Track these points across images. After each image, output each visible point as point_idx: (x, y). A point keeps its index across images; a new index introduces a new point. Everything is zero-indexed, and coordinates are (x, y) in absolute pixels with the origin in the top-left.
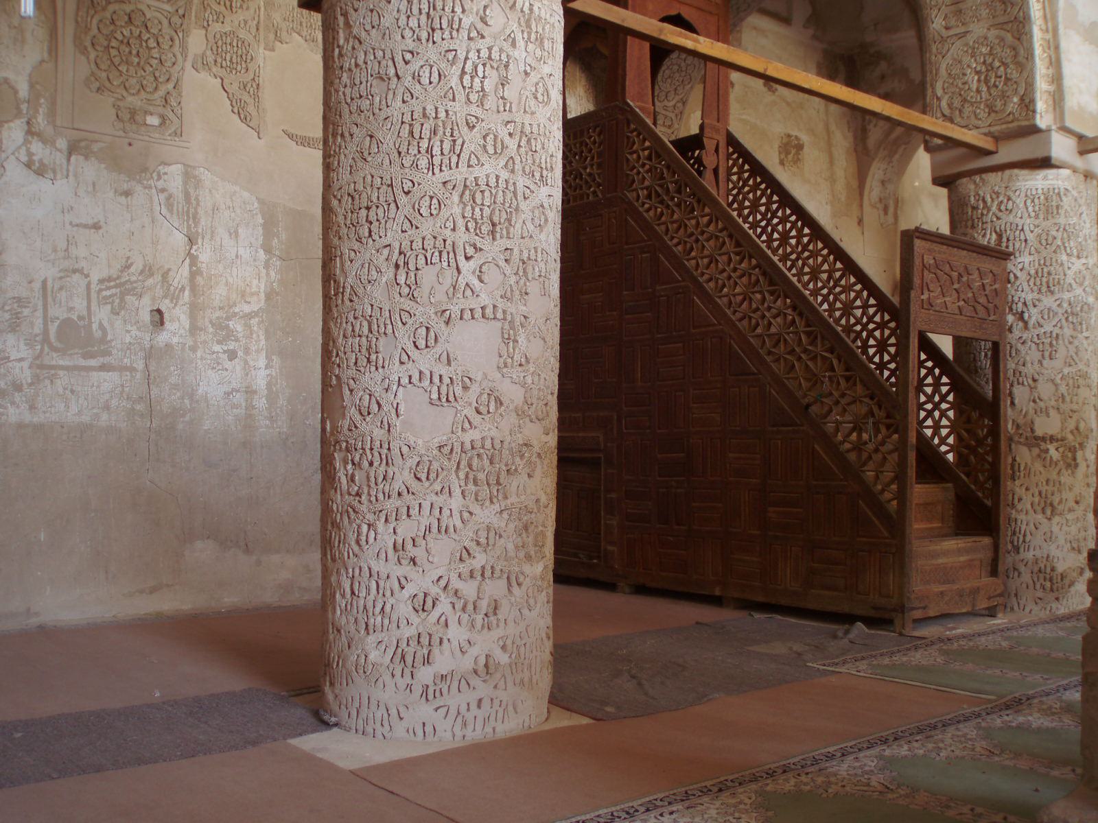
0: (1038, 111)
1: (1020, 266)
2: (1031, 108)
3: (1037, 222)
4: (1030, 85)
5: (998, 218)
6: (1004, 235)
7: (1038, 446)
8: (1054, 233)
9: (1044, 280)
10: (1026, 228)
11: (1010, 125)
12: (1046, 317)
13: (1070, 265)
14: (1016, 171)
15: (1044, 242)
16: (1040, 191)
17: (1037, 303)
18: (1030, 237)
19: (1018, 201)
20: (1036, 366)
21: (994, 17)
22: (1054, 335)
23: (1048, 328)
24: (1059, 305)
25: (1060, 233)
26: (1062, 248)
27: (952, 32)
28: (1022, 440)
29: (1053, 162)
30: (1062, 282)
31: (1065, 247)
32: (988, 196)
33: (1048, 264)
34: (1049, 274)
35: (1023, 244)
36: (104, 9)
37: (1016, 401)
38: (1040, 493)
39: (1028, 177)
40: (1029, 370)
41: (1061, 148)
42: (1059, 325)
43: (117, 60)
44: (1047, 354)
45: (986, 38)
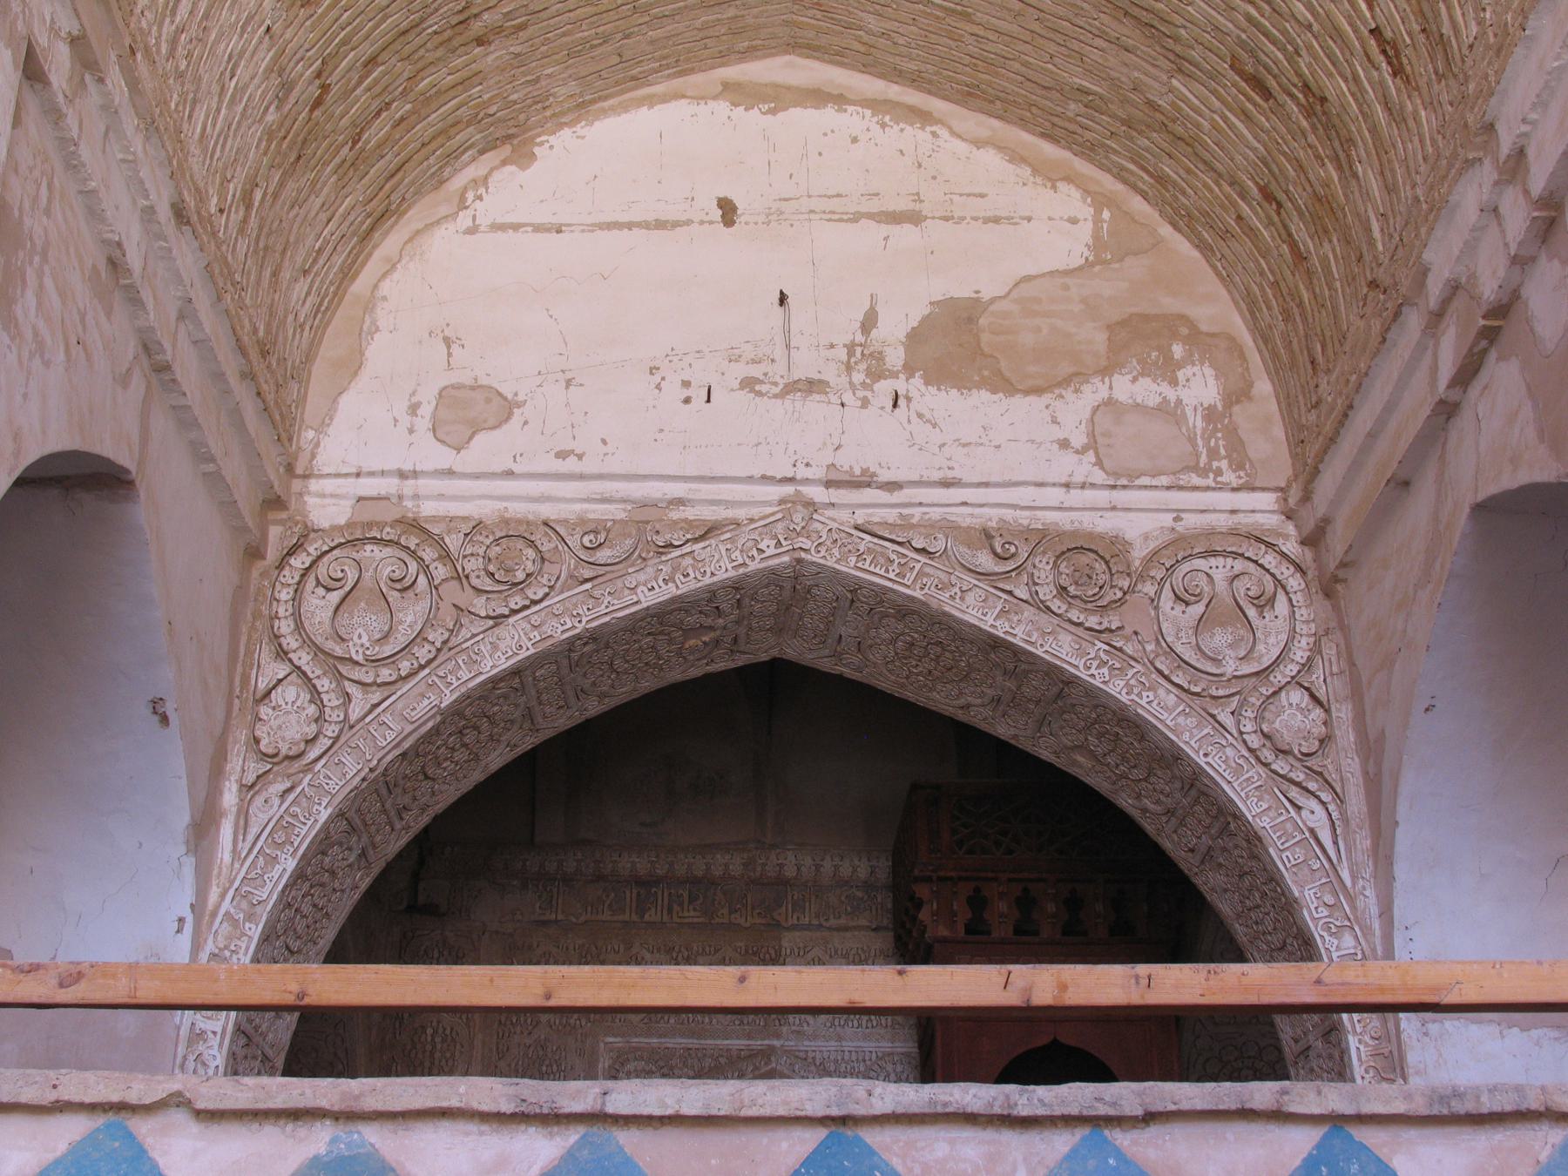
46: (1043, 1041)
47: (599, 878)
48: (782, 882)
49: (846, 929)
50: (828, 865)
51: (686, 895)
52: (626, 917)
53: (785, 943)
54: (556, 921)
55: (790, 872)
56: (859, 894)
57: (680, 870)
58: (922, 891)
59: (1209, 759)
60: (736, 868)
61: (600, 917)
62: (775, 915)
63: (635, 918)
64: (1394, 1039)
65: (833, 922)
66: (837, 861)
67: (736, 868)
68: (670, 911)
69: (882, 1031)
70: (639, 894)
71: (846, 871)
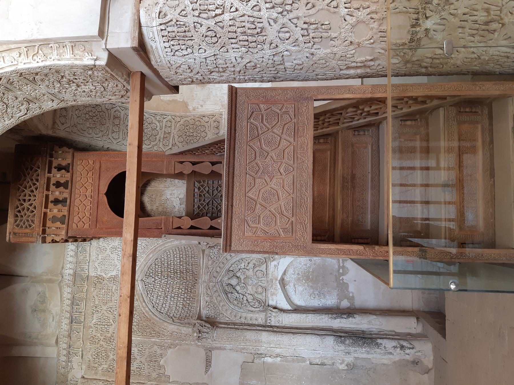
0: (92, 62)
1: (239, 60)
2: (93, 67)
3: (196, 47)
4: (72, 67)
5: (198, 73)
6: (212, 70)
7: (419, 40)
8: (203, 30)
9: (250, 39)
10: (204, 55)
11: (114, 75)
12: (288, 35)
13: (233, 9)
14: (153, 63)
15: (215, 40)
16: (167, 45)
17: (274, 45)
18: (210, 52)
19: (181, 62)
20: (336, 43)
21: (27, 85)
22: (305, 26)
23: (298, 33)
24: (275, 21)
25: (204, 22)
26: (218, 19)
27: (54, 99)
28: (411, 54)
29: (136, 44)
30: (252, 19)
31: (216, 15)
32: (180, 76)
33: (234, 35)
34: (244, 33)
35: (218, 56)
37: (370, 58)
38: (473, 35)
39: (156, 55)
40: (339, 50)
41: (122, 39)
42: (295, 21)
44: (325, 35)
46: (105, 199)
47: (69, 336)
48: (75, 275)
49: (90, 254)
50: (70, 259)
53: (93, 275)
55: (71, 272)
57: (68, 309)
60: (69, 290)
62: (84, 277)
63: (82, 324)
64: (19, 45)
65: (88, 258)
66: (69, 256)
67: (69, 290)
71: (72, 253)
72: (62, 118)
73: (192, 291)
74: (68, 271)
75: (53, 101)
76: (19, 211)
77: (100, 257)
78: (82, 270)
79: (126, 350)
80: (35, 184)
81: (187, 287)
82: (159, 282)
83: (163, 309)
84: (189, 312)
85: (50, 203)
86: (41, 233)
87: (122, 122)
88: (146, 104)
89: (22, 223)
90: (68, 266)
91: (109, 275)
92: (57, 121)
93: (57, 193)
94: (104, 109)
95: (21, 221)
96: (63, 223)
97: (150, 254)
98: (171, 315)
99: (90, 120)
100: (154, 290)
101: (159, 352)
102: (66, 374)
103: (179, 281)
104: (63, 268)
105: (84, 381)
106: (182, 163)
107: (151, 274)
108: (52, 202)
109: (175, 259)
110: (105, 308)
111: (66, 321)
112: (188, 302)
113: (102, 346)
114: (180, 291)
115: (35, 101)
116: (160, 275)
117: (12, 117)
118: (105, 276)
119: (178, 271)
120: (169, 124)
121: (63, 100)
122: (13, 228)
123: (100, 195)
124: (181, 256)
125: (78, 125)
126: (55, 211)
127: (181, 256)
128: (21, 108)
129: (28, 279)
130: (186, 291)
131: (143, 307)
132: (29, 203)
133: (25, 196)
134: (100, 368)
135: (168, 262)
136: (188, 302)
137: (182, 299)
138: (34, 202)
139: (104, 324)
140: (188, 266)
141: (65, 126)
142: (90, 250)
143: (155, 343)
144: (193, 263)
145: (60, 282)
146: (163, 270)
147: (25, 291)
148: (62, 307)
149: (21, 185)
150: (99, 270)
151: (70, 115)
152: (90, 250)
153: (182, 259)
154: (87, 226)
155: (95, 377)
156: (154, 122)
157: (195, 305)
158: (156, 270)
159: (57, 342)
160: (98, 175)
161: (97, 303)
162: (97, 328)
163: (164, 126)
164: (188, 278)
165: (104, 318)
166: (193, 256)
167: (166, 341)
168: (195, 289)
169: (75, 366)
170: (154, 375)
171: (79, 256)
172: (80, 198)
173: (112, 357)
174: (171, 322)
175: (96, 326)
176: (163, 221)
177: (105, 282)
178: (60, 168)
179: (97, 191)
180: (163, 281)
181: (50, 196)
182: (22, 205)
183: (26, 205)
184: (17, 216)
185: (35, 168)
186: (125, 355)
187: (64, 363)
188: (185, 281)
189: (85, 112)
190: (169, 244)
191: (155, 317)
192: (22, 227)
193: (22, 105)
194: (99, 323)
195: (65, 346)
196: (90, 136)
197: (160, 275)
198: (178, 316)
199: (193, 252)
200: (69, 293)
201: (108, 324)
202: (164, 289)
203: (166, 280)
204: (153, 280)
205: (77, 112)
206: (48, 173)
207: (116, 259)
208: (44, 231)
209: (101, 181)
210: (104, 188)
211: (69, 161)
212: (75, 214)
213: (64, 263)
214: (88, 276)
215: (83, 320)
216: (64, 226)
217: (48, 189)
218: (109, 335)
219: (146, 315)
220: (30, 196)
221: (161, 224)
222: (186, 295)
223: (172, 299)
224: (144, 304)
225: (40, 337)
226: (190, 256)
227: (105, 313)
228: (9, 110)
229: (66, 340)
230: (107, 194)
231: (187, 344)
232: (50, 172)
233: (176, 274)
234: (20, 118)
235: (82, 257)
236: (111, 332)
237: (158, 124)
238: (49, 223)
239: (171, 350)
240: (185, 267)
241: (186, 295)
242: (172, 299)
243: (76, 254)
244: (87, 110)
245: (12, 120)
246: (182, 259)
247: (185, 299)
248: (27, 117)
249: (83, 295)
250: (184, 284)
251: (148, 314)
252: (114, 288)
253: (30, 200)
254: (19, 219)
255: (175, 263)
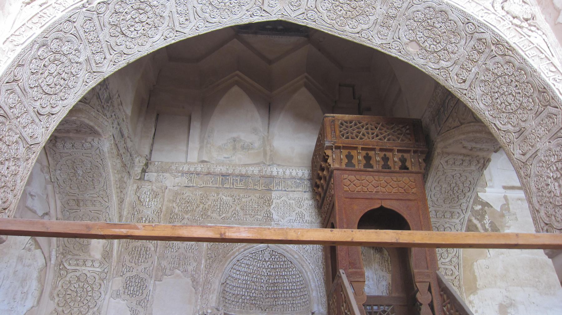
27: (528, 156)
36: (66, 276)
43: (69, 301)
45: (550, 150)
46: (377, 206)
48: (272, 177)
50: (288, 172)
51: (239, 180)
52: (218, 186)
53: (273, 195)
54: (193, 186)
55: (275, 173)
56: (298, 181)
57: (237, 172)
58: (328, 152)
59: (484, 18)
61: (208, 185)
63: (220, 186)
65: (289, 189)
66: (291, 170)
67: (256, 172)
68: (233, 184)
69: (307, 224)
70: (222, 179)
71: (294, 174)
72: (453, 161)
73: (252, 306)
74: (275, 171)
75: (524, 155)
76: (355, 124)
77: (291, 201)
78: (278, 184)
79: (294, 238)
80: (384, 137)
81: (257, 299)
82: (263, 266)
83: (235, 271)
84: (230, 302)
85: (366, 152)
86: (336, 145)
87: (448, 220)
88: (542, 251)
89: (344, 127)
90: (281, 171)
91: (273, 211)
92: (450, 156)
93: (377, 158)
94: (461, 201)
95: (347, 127)
96: (347, 165)
97: (298, 255)
98: (228, 282)
99: (449, 188)
100: (256, 260)
101: (190, 268)
102: (170, 172)
103: (264, 289)
104: (279, 165)
105: (163, 189)
106: (430, 289)
107: (273, 257)
108: (367, 154)
109: (290, 284)
110: (238, 208)
111: (224, 170)
112: (240, 301)
113: (198, 206)
114: (253, 291)
115: (521, 138)
116: (272, 267)
117: (495, 117)
118: (272, 207)
119: (275, 288)
120: (449, 273)
121: (527, 164)
122: (339, 120)
123: (380, 201)
124: (294, 291)
125: (444, 177)
126: (359, 157)
127: (294, 291)
128: (509, 125)
129: (266, 134)
130: (253, 298)
131: (239, 249)
132: (366, 134)
133: (372, 129)
134: (174, 205)
135: (287, 275)
136: (240, 301)
137: (244, 293)
138: (366, 137)
139: (221, 208)
140: (281, 299)
141: (445, 164)
142: (299, 191)
143: (199, 263)
144: (285, 306)
145: (264, 163)
146: (277, 270)
147: (255, 131)
148: (239, 166)
149: (382, 126)
150: (278, 201)
151: (456, 169)
152: (299, 191)
153: (290, 292)
154: (346, 188)
155: (166, 199)
156: (449, 255)
157: (237, 309)
158: (278, 263)
159: (203, 162)
160: (402, 198)
161: (243, 200)
162: (217, 201)
163: (446, 267)
164: (267, 300)
165: (228, 208)
166: (295, 306)
167: (201, 276)
168: (254, 309)
169: (177, 180)
170: (164, 263)
171: (291, 180)
172: (374, 181)
173: (186, 217)
174: (222, 281)
175: (219, 200)
176: (359, 270)
177: (266, 208)
178: (403, 161)
179: (385, 198)
180: (264, 270)
181: (373, 152)
182: (363, 127)
183: (363, 130)
184: (351, 122)
185: (401, 137)
186: (289, 238)
187: (181, 169)
188: (264, 296)
189: (459, 182)
190: (310, 277)
191: (228, 262)
192: (341, 127)
193: (514, 126)
194: (222, 203)
195: (199, 169)
196: (432, 189)
197: (272, 267)
198: (226, 289)
199: (299, 305)
200: (253, 172)
201: (221, 212)
202: (256, 272)
203: (266, 274)
204: (267, 259)
205: (458, 175)
206: (398, 150)
207: (290, 218)
208: (338, 148)
209: (395, 202)
210: (388, 205)
211: (412, 168)
212: (358, 177)
213: (283, 166)
214: (271, 190)
215: (225, 186)
216: (344, 166)
217: (381, 150)
218: (209, 213)
219: (230, 253)
220: (373, 134)
221: (356, 268)
222: (248, 298)
223: (244, 282)
224: (242, 250)
225: (209, 146)
226: (294, 302)
227: (233, 209)
228: (505, 115)
229: (205, 170)
230: (382, 208)
231: (196, 301)
232: (399, 151)
233: (272, 285)
234: (493, 125)
235: (290, 183)
236: (212, 215)
237: (447, 260)
238: (345, 152)
239: (191, 282)
240: (280, 296)
241: (248, 298)
242: (244, 282)
243: (294, 178)
244: (461, 185)
245: (491, 117)
246: (290, 292)
247: (243, 297)
248: (494, 131)
249: (251, 186)
250: (261, 295)
251: (232, 255)
252: (259, 217)
253: (368, 133)
254: (349, 125)
255: (285, 284)
